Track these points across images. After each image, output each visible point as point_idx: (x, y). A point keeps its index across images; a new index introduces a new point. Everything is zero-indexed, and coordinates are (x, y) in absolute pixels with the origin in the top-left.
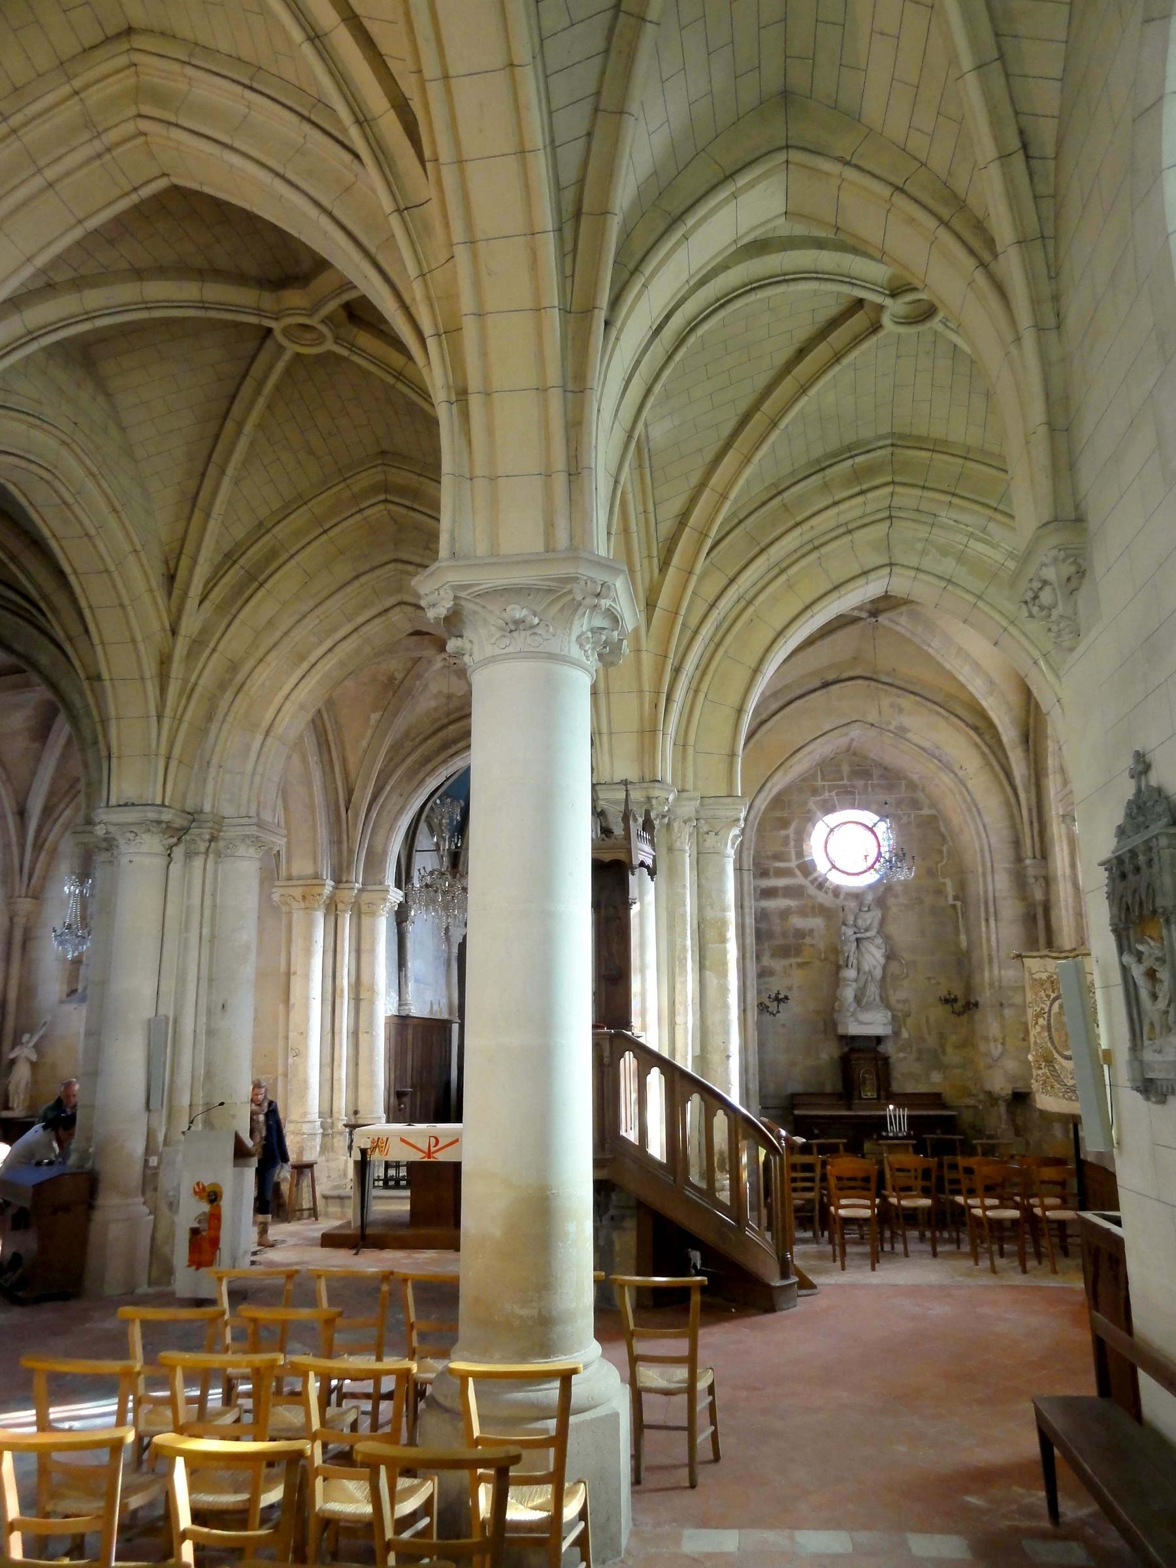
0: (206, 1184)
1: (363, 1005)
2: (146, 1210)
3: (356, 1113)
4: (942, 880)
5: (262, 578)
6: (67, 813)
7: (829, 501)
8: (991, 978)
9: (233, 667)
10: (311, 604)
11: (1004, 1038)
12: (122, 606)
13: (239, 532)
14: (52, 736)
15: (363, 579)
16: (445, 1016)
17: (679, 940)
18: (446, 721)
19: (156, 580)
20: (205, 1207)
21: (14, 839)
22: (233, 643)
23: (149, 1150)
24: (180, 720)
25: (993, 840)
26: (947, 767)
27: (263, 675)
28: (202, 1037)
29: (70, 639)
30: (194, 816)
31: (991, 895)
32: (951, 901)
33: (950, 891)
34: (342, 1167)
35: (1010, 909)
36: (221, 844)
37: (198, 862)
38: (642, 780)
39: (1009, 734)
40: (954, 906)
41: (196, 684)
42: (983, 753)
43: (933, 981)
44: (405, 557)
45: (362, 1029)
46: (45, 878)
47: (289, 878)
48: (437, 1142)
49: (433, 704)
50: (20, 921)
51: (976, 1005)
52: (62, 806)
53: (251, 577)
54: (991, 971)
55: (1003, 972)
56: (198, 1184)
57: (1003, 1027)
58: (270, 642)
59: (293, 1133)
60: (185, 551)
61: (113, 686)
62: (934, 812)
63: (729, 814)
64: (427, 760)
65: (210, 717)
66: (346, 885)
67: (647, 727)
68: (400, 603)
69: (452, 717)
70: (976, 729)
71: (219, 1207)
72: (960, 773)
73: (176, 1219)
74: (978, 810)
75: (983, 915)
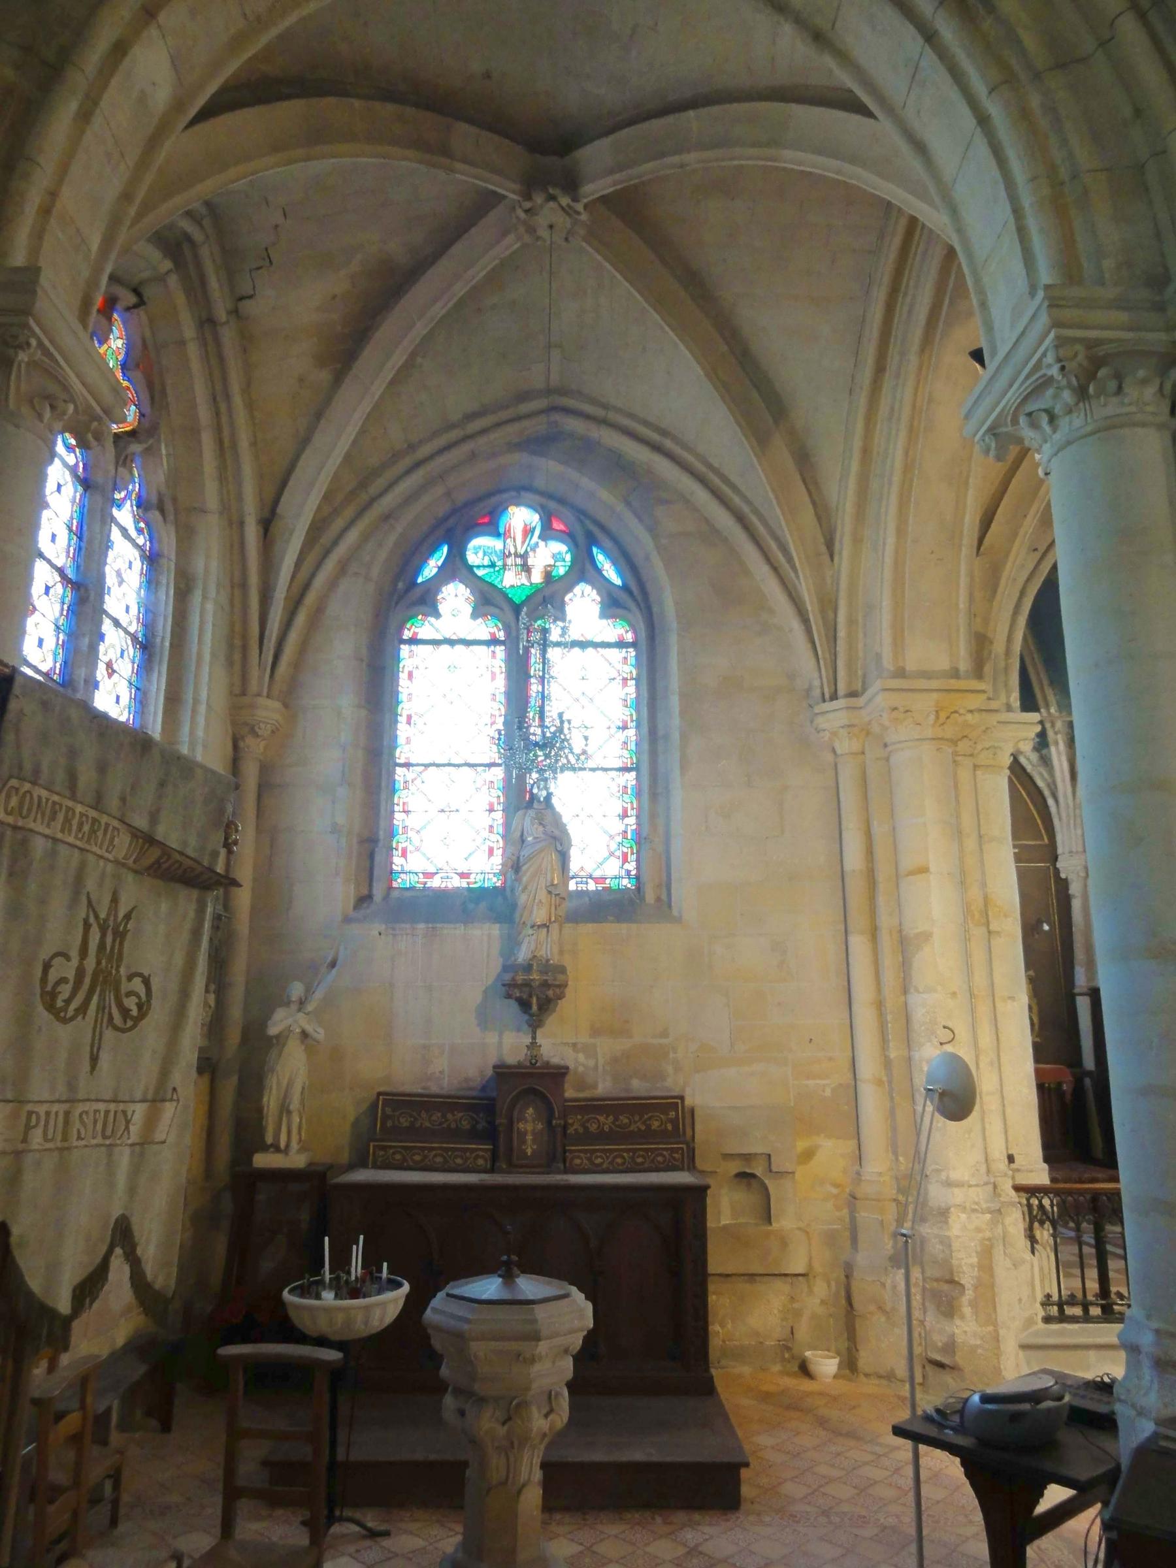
6: (352, 536)
14: (369, 355)
21: (254, 579)
46: (297, 666)
47: (901, 673)
50: (255, 748)
52: (339, 523)
59: (963, 1208)
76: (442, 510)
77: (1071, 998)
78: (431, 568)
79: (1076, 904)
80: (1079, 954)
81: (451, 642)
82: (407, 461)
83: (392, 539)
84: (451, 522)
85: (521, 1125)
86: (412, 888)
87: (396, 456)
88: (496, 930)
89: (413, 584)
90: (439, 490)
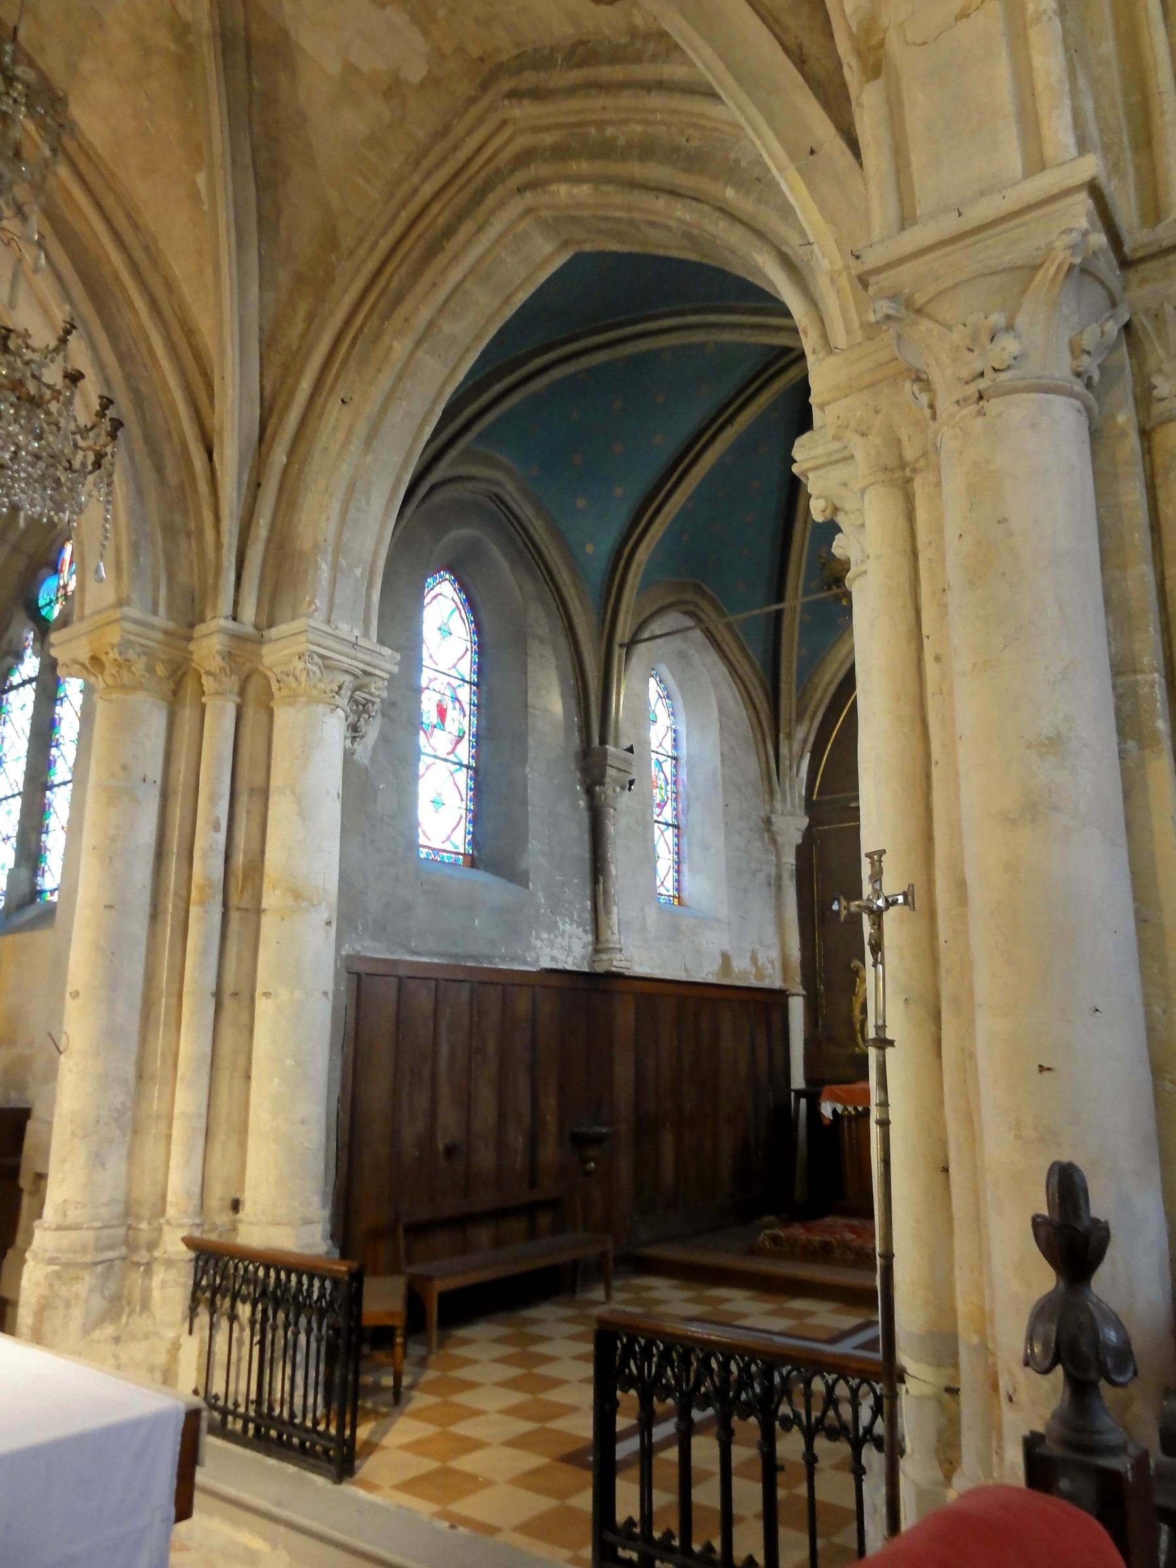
3: (236, 1206)
16: (777, 984)
34: (161, 1358)
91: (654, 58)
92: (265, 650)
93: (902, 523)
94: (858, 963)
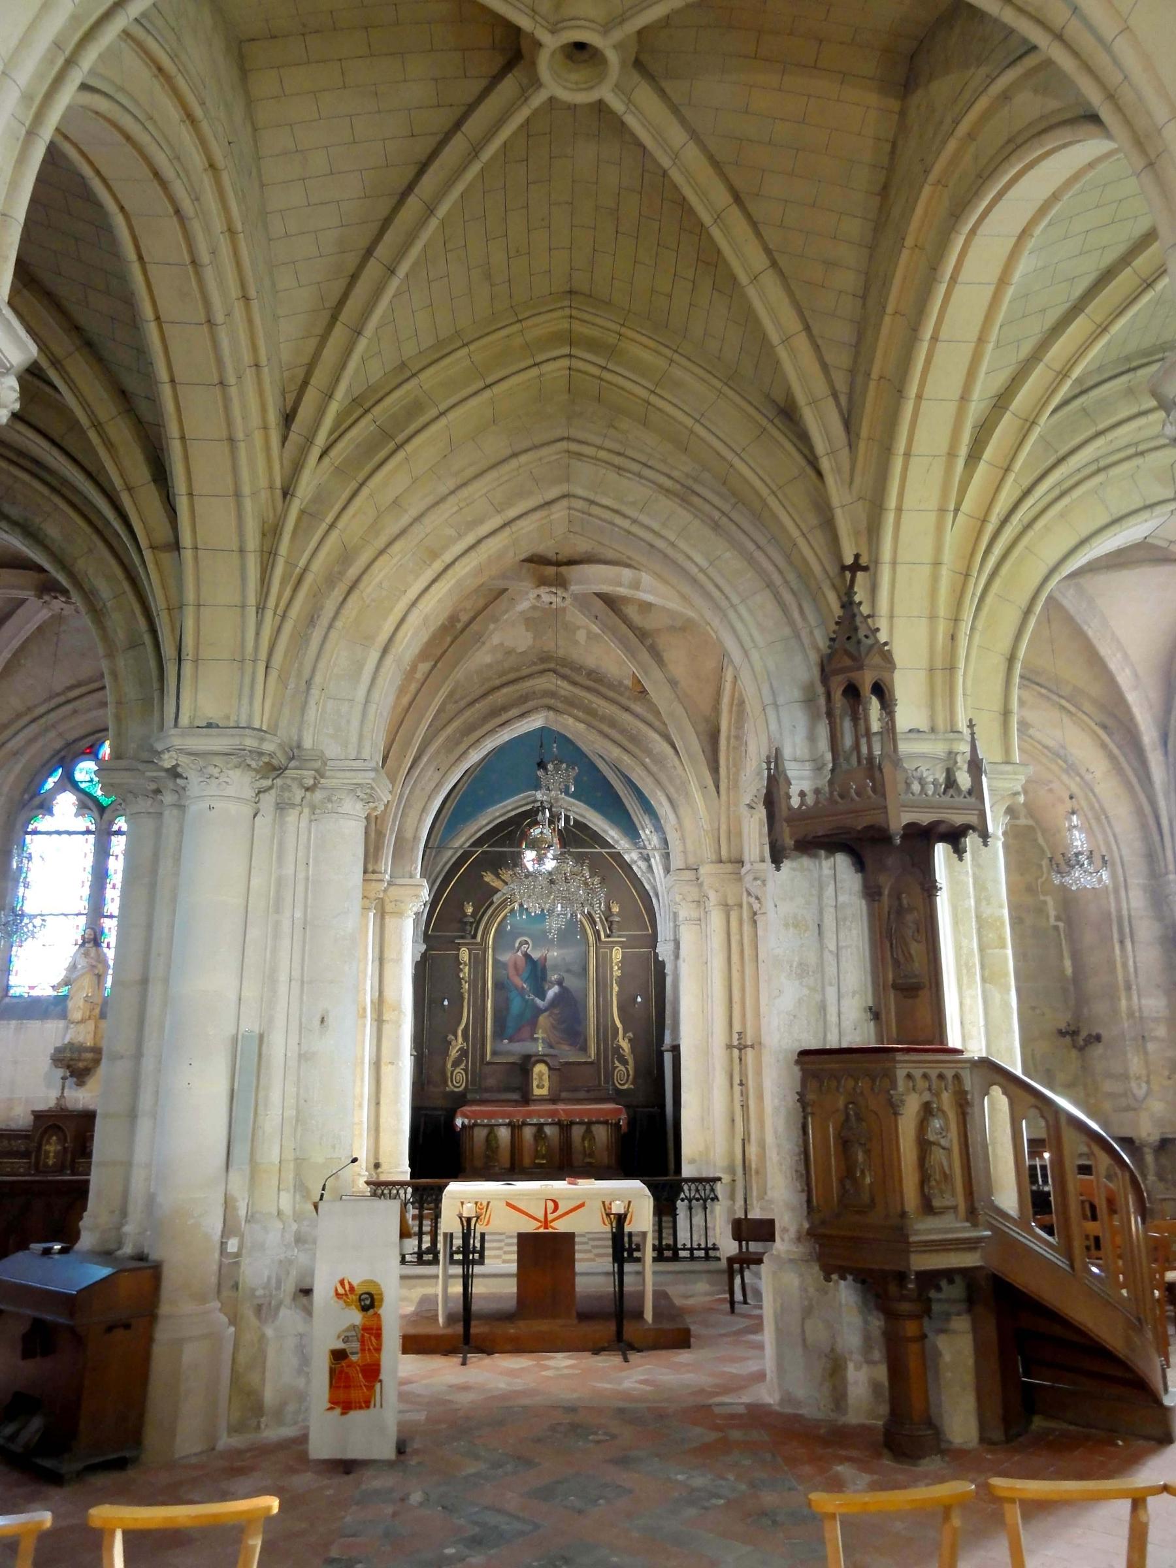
0: (355, 1284)
1: (386, 1028)
2: (224, 1319)
3: (377, 1166)
4: (1042, 898)
5: (400, 438)
7: (1134, 410)
8: (1129, 1008)
9: (346, 557)
10: (451, 484)
11: (1148, 1076)
12: (231, 440)
13: (376, 372)
15: (523, 459)
17: (965, 942)
18: (497, 682)
19: (273, 418)
20: (356, 1317)
22: (353, 523)
23: (228, 1230)
24: (284, 616)
25: (1125, 851)
26: (1071, 769)
27: (382, 571)
28: (292, 1063)
29: (129, 489)
30: (294, 753)
31: (1125, 913)
32: (1052, 921)
33: (1052, 913)
35: (1147, 930)
36: (318, 795)
37: (292, 817)
38: (933, 730)
39: (1149, 735)
40: (1056, 928)
41: (306, 569)
42: (1112, 757)
43: (1038, 1011)
44: (580, 435)
45: (385, 1058)
48: (556, 1208)
49: (488, 659)
51: (1098, 1038)
53: (385, 435)
54: (1129, 998)
55: (1143, 1002)
56: (342, 1283)
57: (1147, 1063)
58: (395, 529)
60: (313, 381)
61: (196, 558)
62: (1030, 822)
63: (1007, 785)
64: (470, 729)
65: (311, 620)
66: (374, 877)
67: (939, 664)
68: (564, 496)
69: (504, 679)
70: (1104, 727)
71: (378, 1316)
72: (1088, 777)
73: (269, 1332)
74: (1107, 817)
75: (1116, 936)
76: (58, 744)
77: (660, 1055)
78: (50, 783)
79: (669, 980)
80: (668, 1021)
81: (58, 833)
82: (27, 718)
83: (18, 768)
84: (63, 753)
85: (48, 1147)
86: (21, 996)
87: (19, 716)
88: (61, 1024)
89: (39, 794)
90: (52, 734)
91: (629, 698)
92: (392, 888)
93: (724, 922)
94: (451, 1037)
